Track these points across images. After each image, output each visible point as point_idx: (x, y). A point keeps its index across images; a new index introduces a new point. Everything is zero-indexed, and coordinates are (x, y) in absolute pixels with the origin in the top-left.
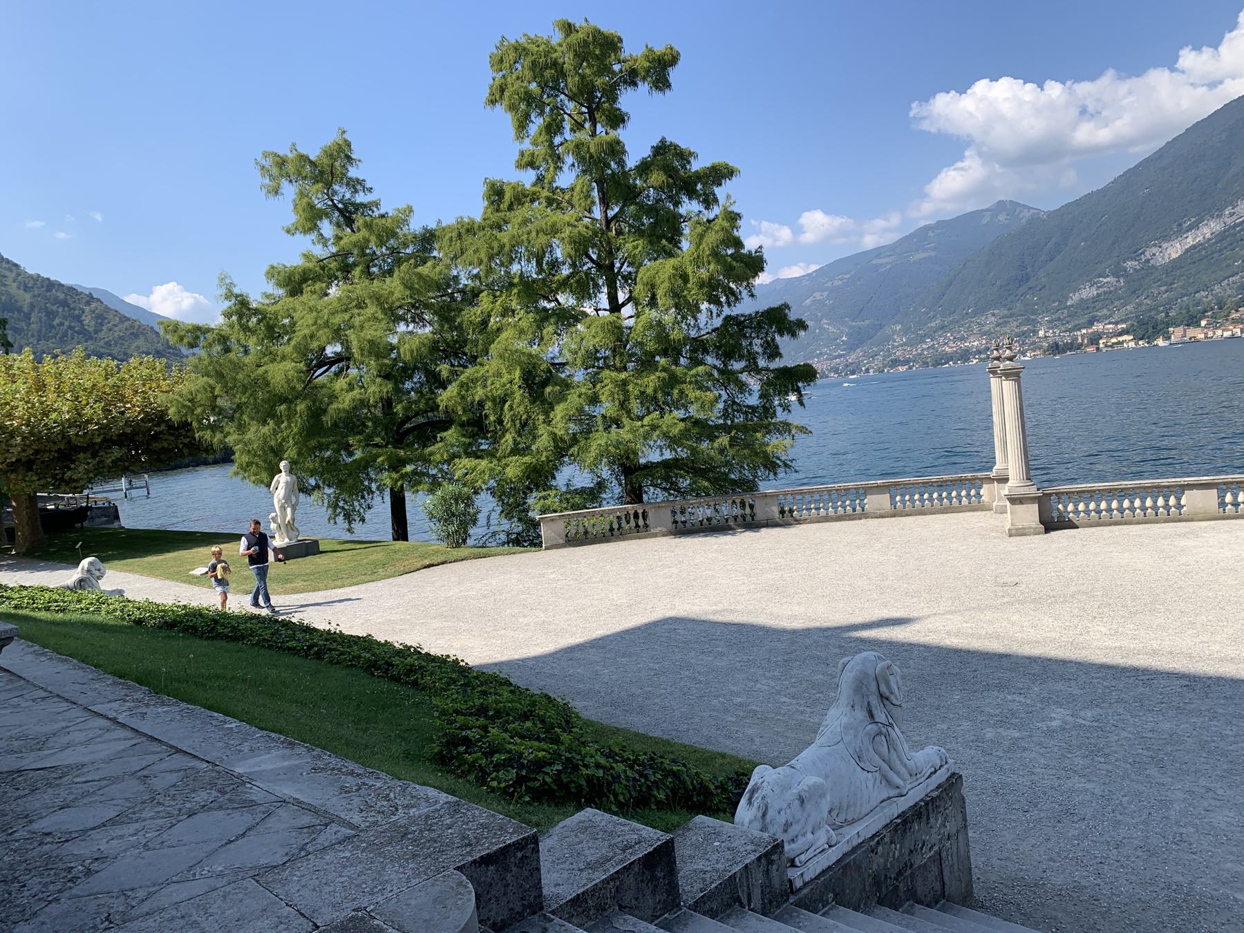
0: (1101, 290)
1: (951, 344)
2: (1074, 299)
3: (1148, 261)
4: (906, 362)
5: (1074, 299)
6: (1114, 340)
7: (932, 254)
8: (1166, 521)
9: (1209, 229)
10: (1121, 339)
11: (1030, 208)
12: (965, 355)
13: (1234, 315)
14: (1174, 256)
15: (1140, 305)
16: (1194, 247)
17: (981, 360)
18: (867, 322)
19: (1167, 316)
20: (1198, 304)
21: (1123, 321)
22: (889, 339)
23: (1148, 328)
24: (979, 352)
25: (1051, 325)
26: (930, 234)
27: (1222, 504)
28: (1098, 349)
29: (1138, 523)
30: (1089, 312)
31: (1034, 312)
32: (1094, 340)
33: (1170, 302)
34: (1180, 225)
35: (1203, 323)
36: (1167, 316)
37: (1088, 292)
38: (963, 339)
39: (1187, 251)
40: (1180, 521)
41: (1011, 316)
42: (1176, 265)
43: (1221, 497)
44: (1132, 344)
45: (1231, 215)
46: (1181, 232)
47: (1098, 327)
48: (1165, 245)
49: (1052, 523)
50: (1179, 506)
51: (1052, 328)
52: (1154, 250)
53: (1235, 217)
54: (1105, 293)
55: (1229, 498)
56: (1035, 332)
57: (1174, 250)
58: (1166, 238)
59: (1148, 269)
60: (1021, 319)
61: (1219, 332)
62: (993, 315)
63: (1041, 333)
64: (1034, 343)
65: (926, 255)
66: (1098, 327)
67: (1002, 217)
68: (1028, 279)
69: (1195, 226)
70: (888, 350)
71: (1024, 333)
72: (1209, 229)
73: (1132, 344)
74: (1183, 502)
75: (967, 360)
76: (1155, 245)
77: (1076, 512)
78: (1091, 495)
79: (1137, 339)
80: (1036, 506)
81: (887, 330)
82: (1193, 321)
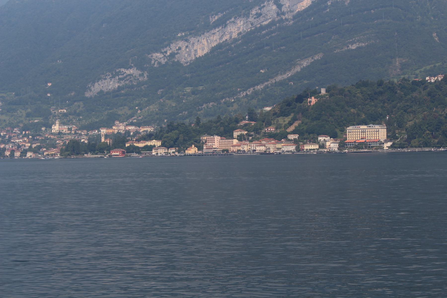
0: (123, 83)
3: (173, 55)
14: (200, 53)
16: (219, 46)
30: (107, 108)
37: (109, 84)
39: (213, 50)
42: (199, 63)
45: (259, 15)
46: (208, 27)
48: (192, 40)
52: (181, 44)
53: (262, 19)
56: (49, 127)
63: (56, 128)
69: (222, 23)
72: (236, 28)
76: (182, 38)
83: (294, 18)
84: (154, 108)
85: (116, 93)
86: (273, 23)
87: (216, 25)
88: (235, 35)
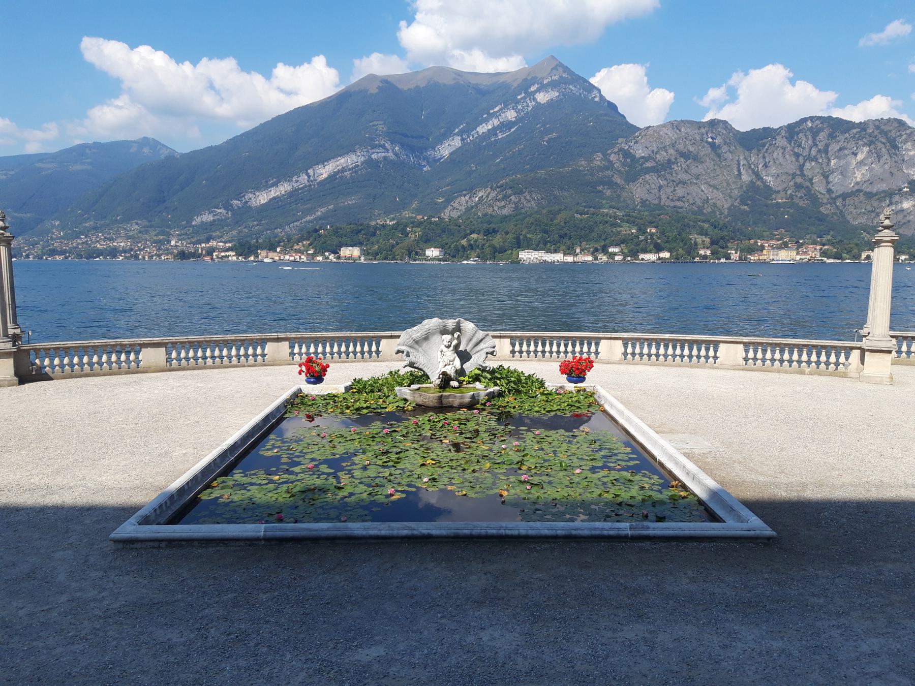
0: (216, 217)
1: (102, 242)
2: (197, 221)
3: (246, 202)
4: (63, 252)
5: (197, 221)
6: (223, 254)
7: (89, 167)
8: (127, 373)
9: (283, 188)
10: (227, 254)
11: (167, 148)
12: (114, 253)
13: (296, 247)
14: (263, 202)
15: (241, 232)
16: (274, 198)
17: (126, 257)
18: (29, 215)
19: (257, 242)
20: (276, 237)
21: (230, 242)
22: (48, 231)
23: (245, 248)
24: (125, 251)
25: (180, 237)
26: (87, 151)
27: (169, 360)
28: (212, 259)
29: (104, 375)
30: (207, 232)
31: (169, 227)
32: (210, 252)
33: (260, 233)
34: (267, 182)
35: (278, 249)
36: (257, 242)
37: (207, 218)
38: (112, 239)
39: (271, 200)
40: (137, 373)
41: (151, 226)
43: (168, 354)
44: (235, 258)
46: (267, 187)
47: (213, 243)
48: (257, 194)
49: (26, 374)
50: (137, 361)
51: (181, 240)
52: (251, 195)
54: (218, 220)
55: (174, 355)
56: (169, 242)
57: (262, 198)
58: (259, 189)
59: (246, 209)
60: (158, 230)
61: (287, 257)
62: (137, 224)
63: (173, 243)
64: (167, 249)
65: (83, 167)
66: (213, 243)
67: (146, 150)
68: (164, 201)
69: (275, 184)
70: (47, 241)
71: (160, 241)
72: (283, 188)
73: (235, 258)
74: (140, 358)
75: (115, 256)
76: (251, 192)
77: (52, 366)
78: (67, 351)
79: (238, 255)
80: (11, 361)
81: (47, 224)
82: (272, 248)
83: (318, 184)
84: (234, 232)
85: (212, 224)
86: (306, 186)
87: (272, 185)
88: (283, 192)
